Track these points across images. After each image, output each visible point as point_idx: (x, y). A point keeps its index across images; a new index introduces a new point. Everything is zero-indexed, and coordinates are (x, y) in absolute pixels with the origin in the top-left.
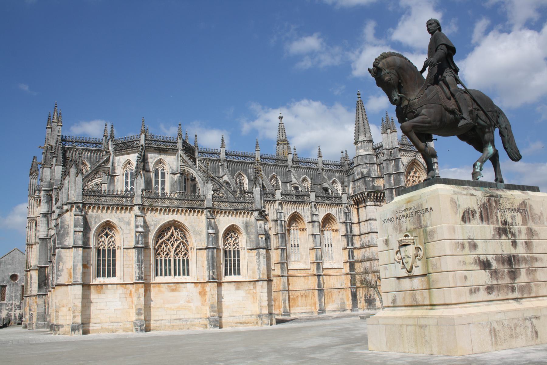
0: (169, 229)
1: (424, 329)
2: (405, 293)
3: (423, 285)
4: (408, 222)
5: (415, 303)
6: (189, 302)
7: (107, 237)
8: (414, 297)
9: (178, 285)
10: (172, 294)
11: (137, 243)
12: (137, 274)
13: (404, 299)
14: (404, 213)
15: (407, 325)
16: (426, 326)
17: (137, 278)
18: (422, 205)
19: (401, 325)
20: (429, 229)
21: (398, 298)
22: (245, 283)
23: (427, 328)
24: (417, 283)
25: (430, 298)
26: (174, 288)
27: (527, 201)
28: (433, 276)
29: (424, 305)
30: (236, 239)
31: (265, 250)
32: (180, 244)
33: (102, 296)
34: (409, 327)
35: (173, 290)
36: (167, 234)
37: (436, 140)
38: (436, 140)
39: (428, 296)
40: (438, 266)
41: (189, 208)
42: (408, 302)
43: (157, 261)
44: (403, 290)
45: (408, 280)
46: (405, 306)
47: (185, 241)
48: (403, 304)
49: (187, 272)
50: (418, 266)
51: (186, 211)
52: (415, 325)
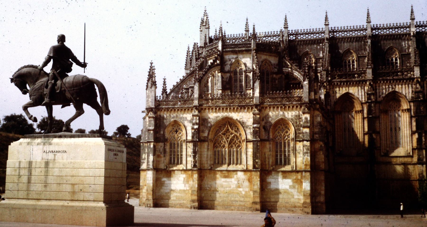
0: (225, 125)
6: (239, 187)
7: (177, 133)
9: (230, 173)
10: (223, 180)
11: (193, 137)
12: (192, 162)
17: (193, 166)
22: (293, 173)
26: (226, 175)
30: (287, 132)
31: (309, 142)
32: (234, 137)
33: (172, 179)
35: (225, 177)
36: (223, 129)
41: (239, 106)
43: (215, 152)
47: (238, 135)
49: (238, 162)
51: (237, 108)
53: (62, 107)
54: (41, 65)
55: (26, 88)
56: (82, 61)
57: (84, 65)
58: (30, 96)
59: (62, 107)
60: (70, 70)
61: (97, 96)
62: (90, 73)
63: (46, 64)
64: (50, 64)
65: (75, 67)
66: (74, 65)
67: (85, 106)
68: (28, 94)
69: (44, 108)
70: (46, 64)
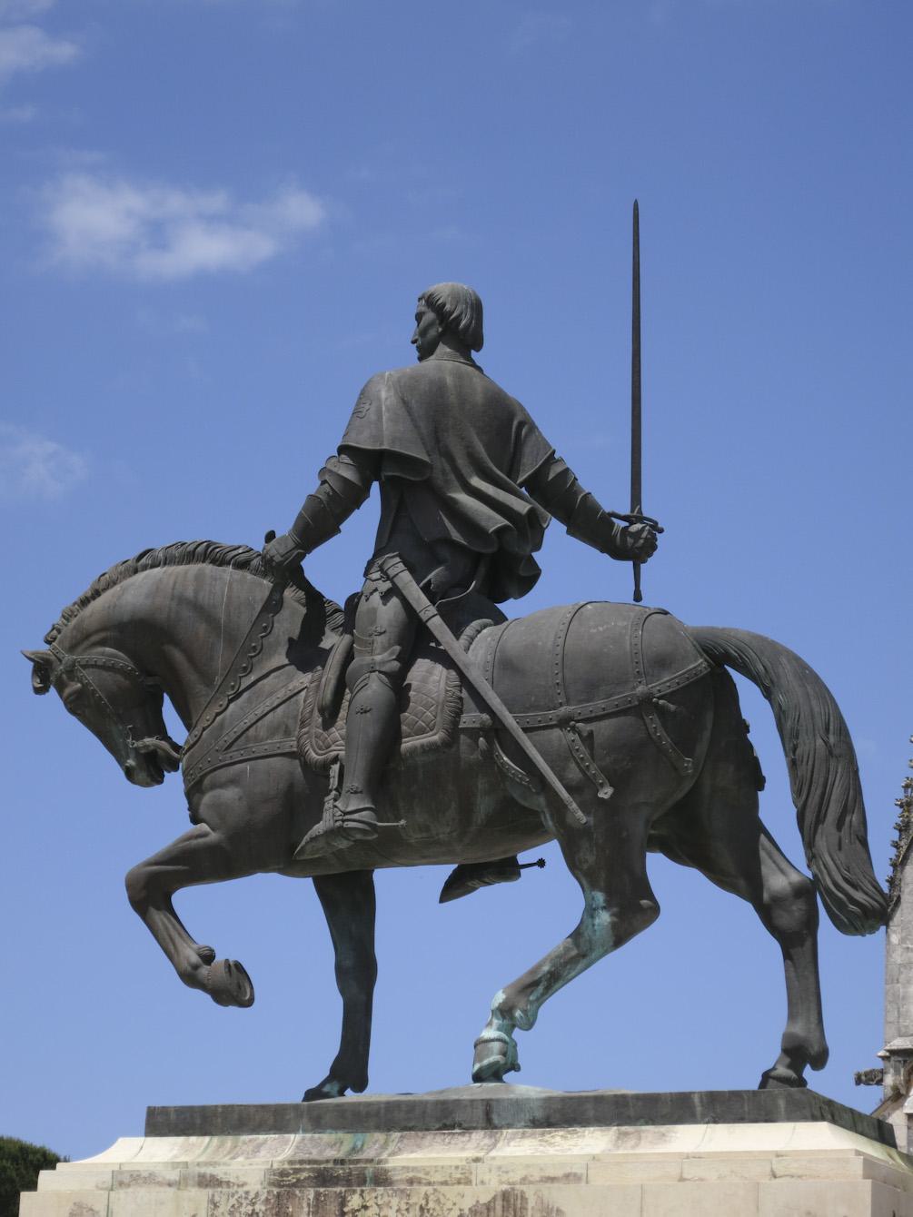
27: (530, 1192)
37: (541, 863)
38: (541, 863)
53: (453, 889)
54: (285, 528)
55: (161, 731)
56: (611, 497)
57: (630, 542)
58: (194, 791)
59: (453, 889)
60: (526, 579)
61: (757, 781)
62: (696, 589)
63: (320, 523)
64: (366, 520)
65: (559, 549)
66: (555, 531)
67: (661, 870)
68: (174, 782)
69: (304, 888)
70: (320, 523)
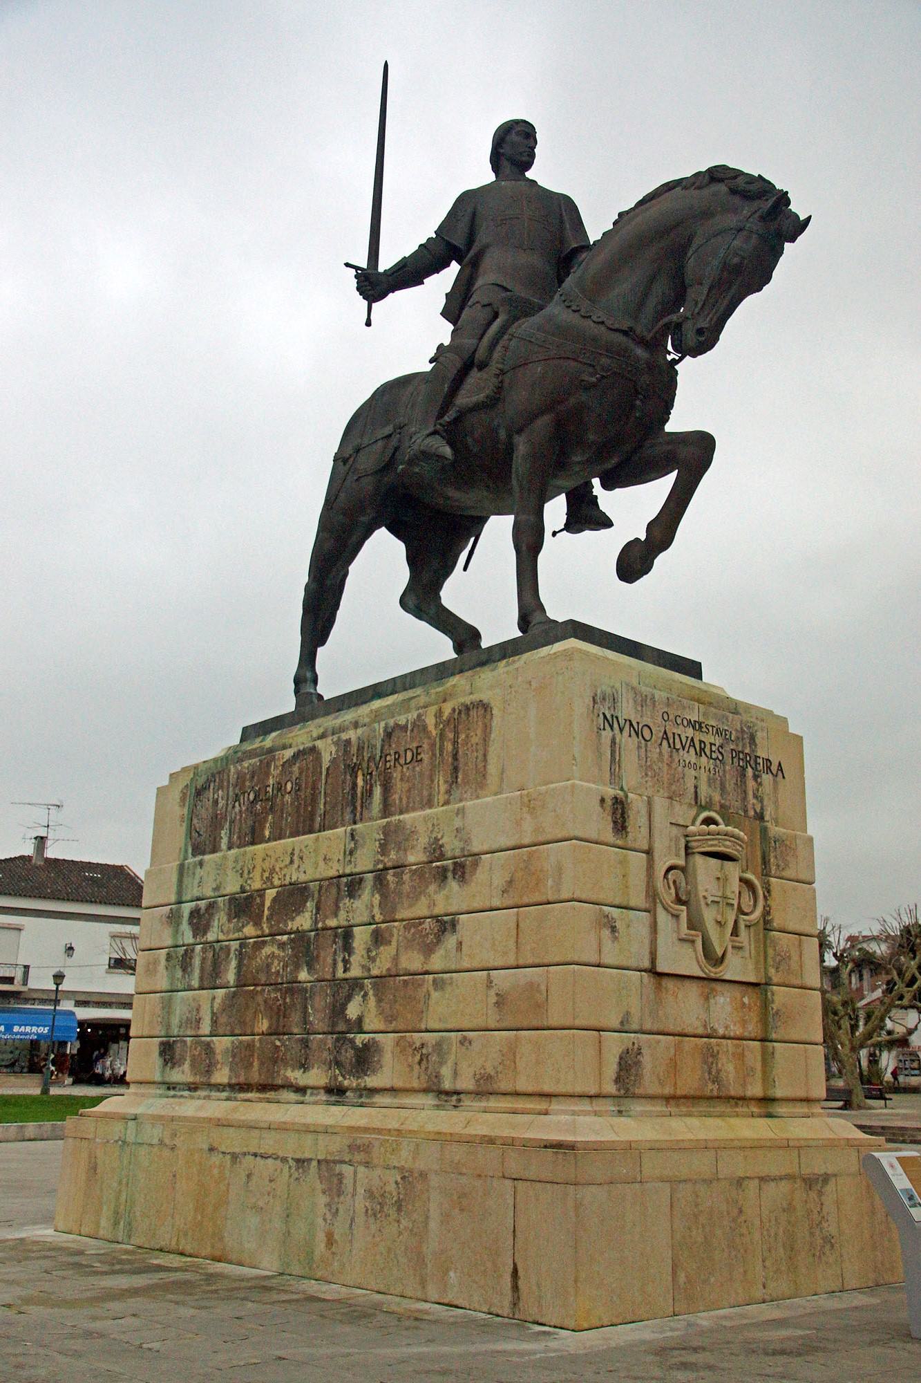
1: (820, 1193)
2: (678, 1047)
3: (744, 1023)
4: (704, 777)
5: (711, 1088)
8: (710, 1057)
13: (674, 1066)
14: (690, 732)
15: (762, 1179)
16: (826, 1178)
18: (752, 738)
19: (740, 1182)
20: (775, 830)
21: (646, 1060)
23: (830, 1188)
24: (724, 1010)
25: (767, 1079)
28: (780, 995)
29: (743, 1098)
34: (771, 1189)
39: (759, 1066)
40: (794, 965)
42: (690, 1081)
44: (671, 1028)
45: (692, 992)
46: (668, 1099)
48: (668, 1090)
50: (740, 948)
52: (790, 1177)
